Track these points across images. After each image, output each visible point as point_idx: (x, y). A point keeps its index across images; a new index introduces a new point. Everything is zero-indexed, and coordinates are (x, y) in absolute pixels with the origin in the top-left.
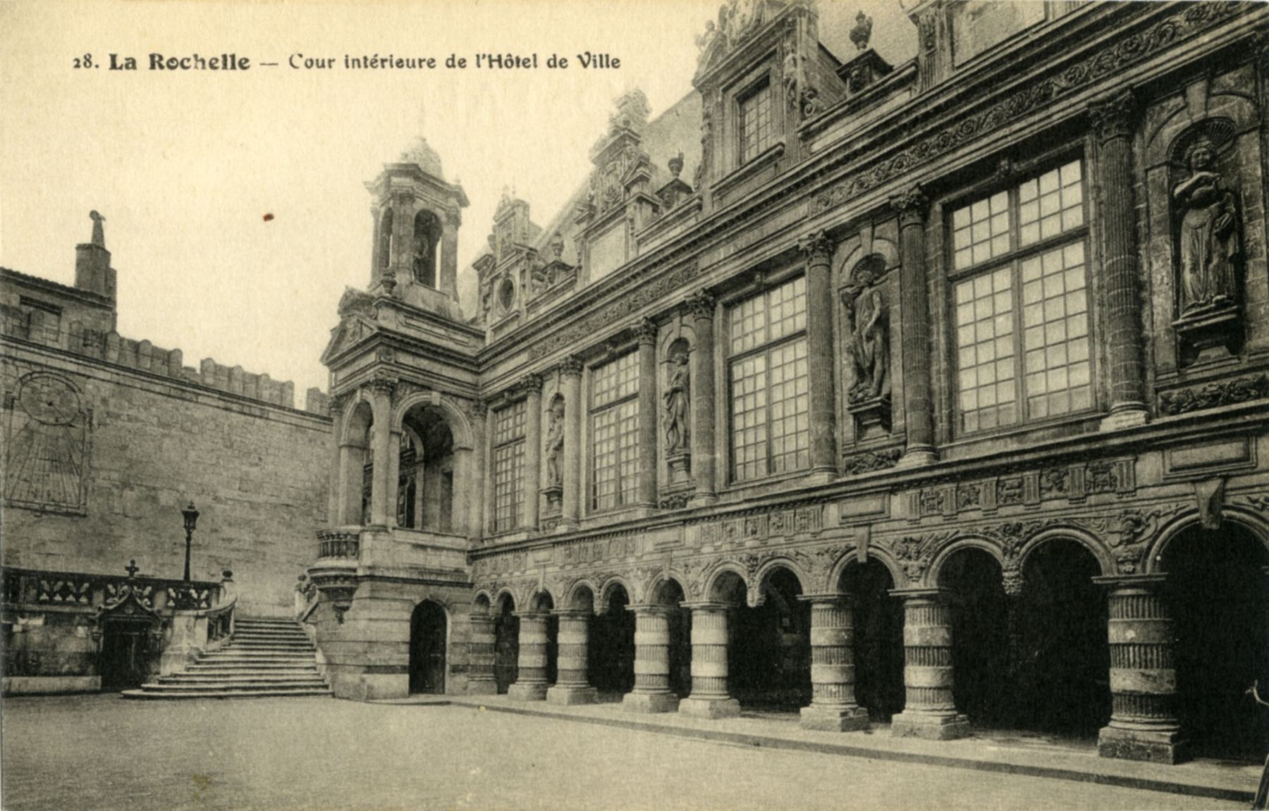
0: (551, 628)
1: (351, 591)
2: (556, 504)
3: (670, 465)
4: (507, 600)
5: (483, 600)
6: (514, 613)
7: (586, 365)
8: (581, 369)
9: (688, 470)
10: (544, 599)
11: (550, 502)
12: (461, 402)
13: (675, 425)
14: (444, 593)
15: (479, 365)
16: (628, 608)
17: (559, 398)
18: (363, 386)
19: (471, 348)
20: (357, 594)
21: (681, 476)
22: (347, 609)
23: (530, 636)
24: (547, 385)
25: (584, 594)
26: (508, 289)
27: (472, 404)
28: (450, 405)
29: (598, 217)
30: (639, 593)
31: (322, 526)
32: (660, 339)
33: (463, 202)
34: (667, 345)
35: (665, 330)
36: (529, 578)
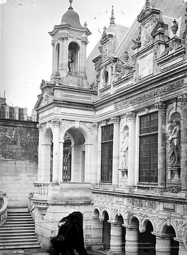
0: (123, 230)
1: (46, 209)
2: (125, 175)
3: (172, 171)
4: (106, 214)
5: (97, 211)
6: (109, 221)
7: (138, 115)
8: (135, 117)
9: (179, 174)
10: (120, 218)
11: (123, 175)
12: (88, 124)
13: (173, 154)
14: (81, 209)
15: (95, 108)
16: (153, 233)
17: (126, 128)
18: (50, 121)
19: (92, 99)
20: (48, 210)
21: (176, 177)
22: (44, 215)
23: (115, 232)
24: (122, 120)
25: (135, 221)
26: (107, 74)
27: (92, 124)
28: (82, 126)
29: (142, 47)
30: (158, 230)
31: (36, 182)
32: (168, 110)
33: (88, 33)
34: (170, 116)
35: (170, 106)
36: (114, 208)
